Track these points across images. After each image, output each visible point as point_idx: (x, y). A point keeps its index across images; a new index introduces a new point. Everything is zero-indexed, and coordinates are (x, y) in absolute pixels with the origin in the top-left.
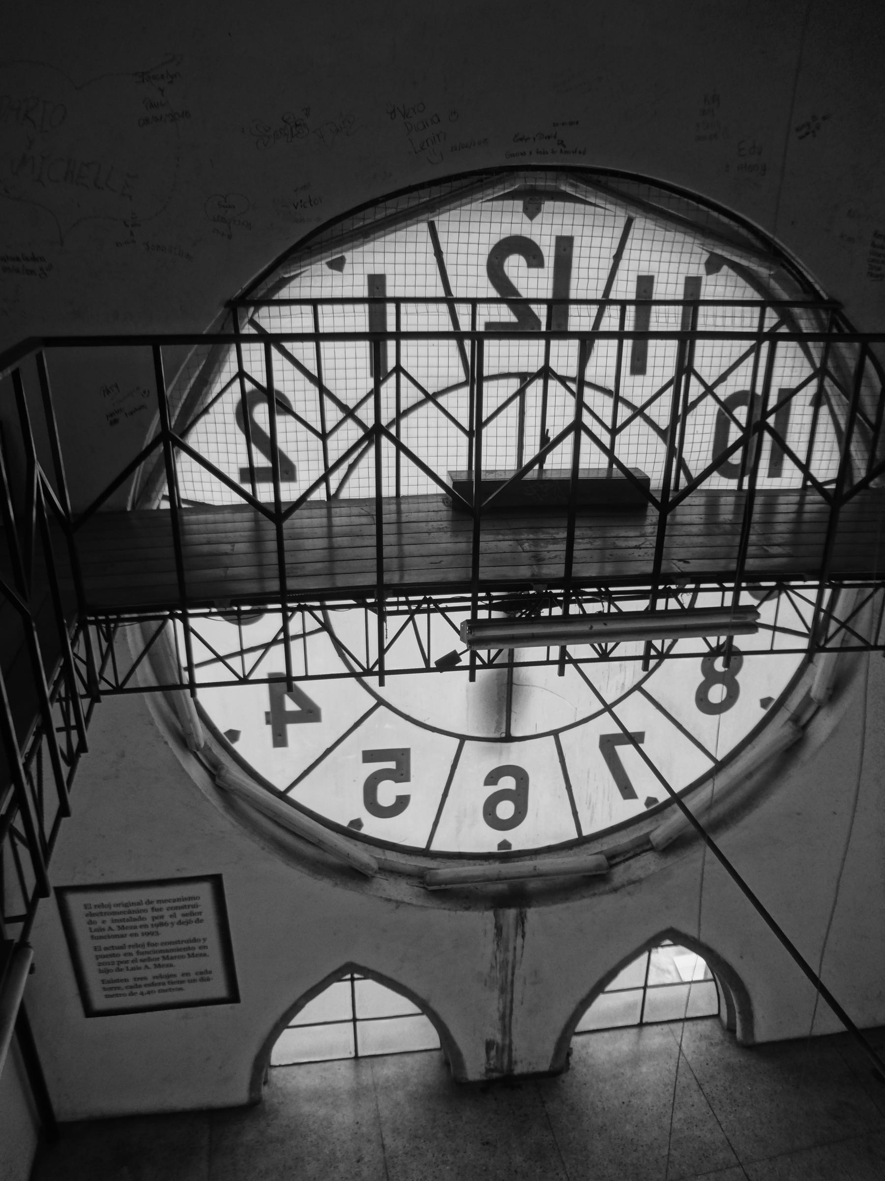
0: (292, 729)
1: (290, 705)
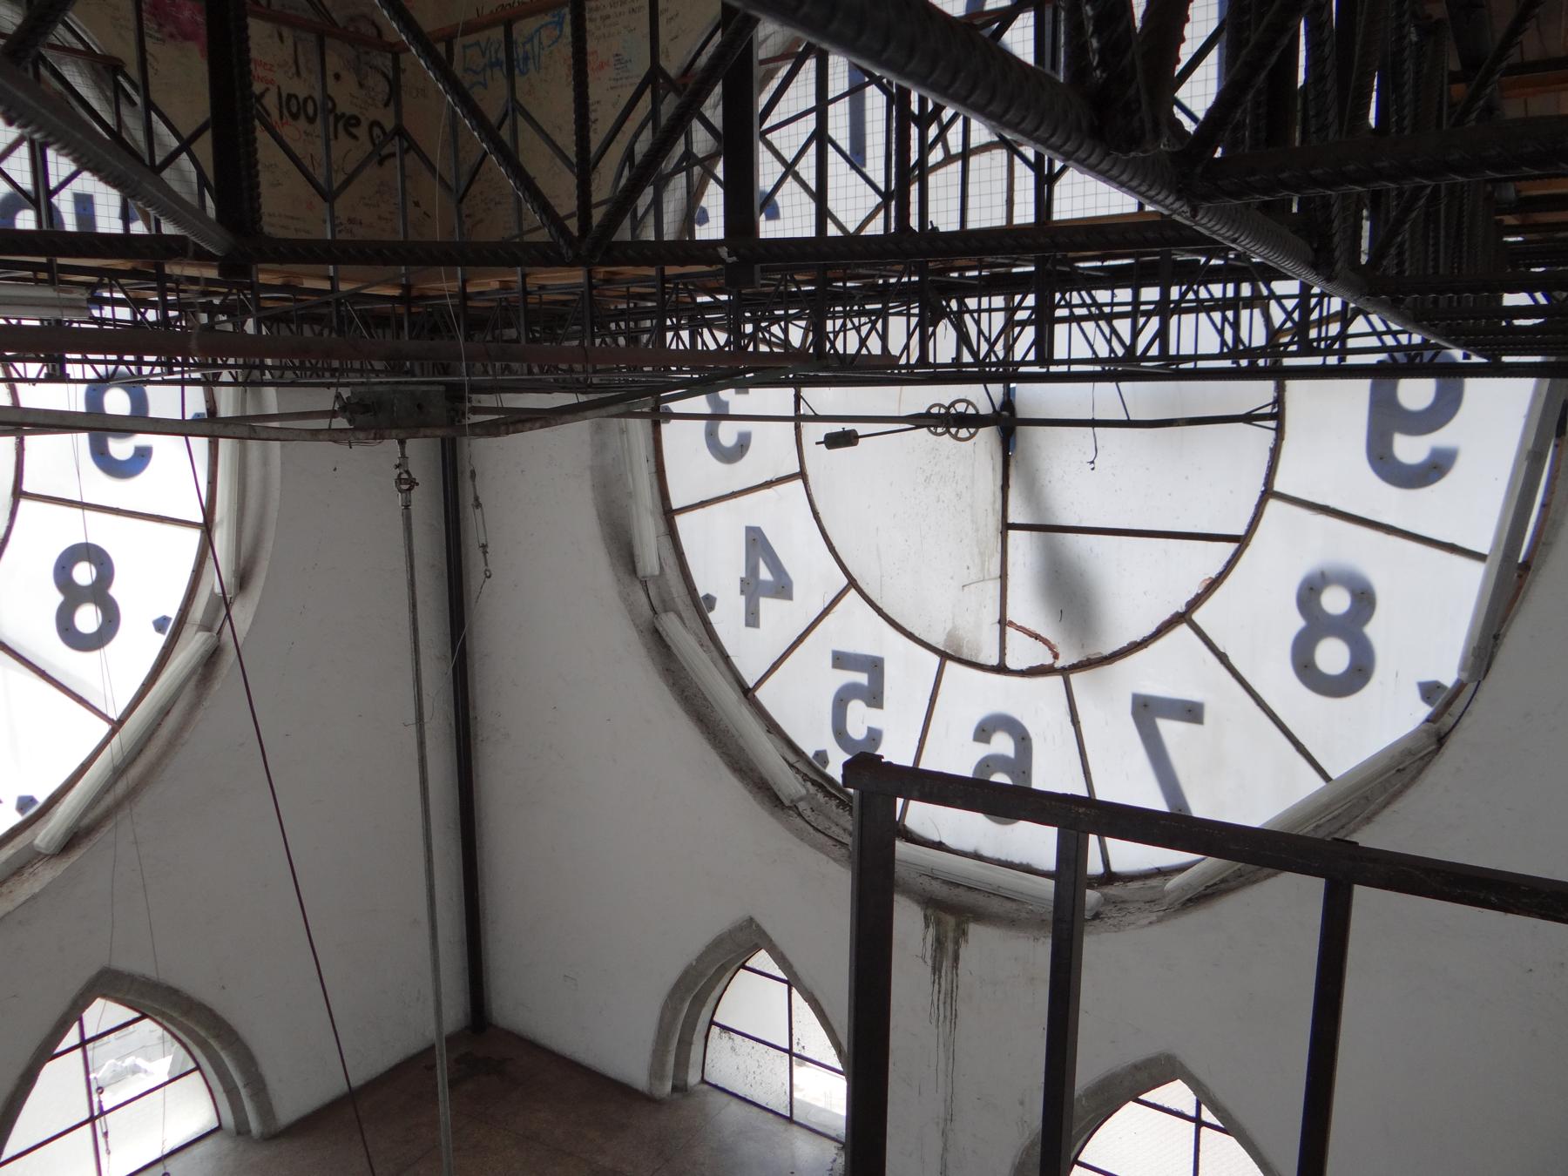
0: (767, 605)
1: (765, 574)
